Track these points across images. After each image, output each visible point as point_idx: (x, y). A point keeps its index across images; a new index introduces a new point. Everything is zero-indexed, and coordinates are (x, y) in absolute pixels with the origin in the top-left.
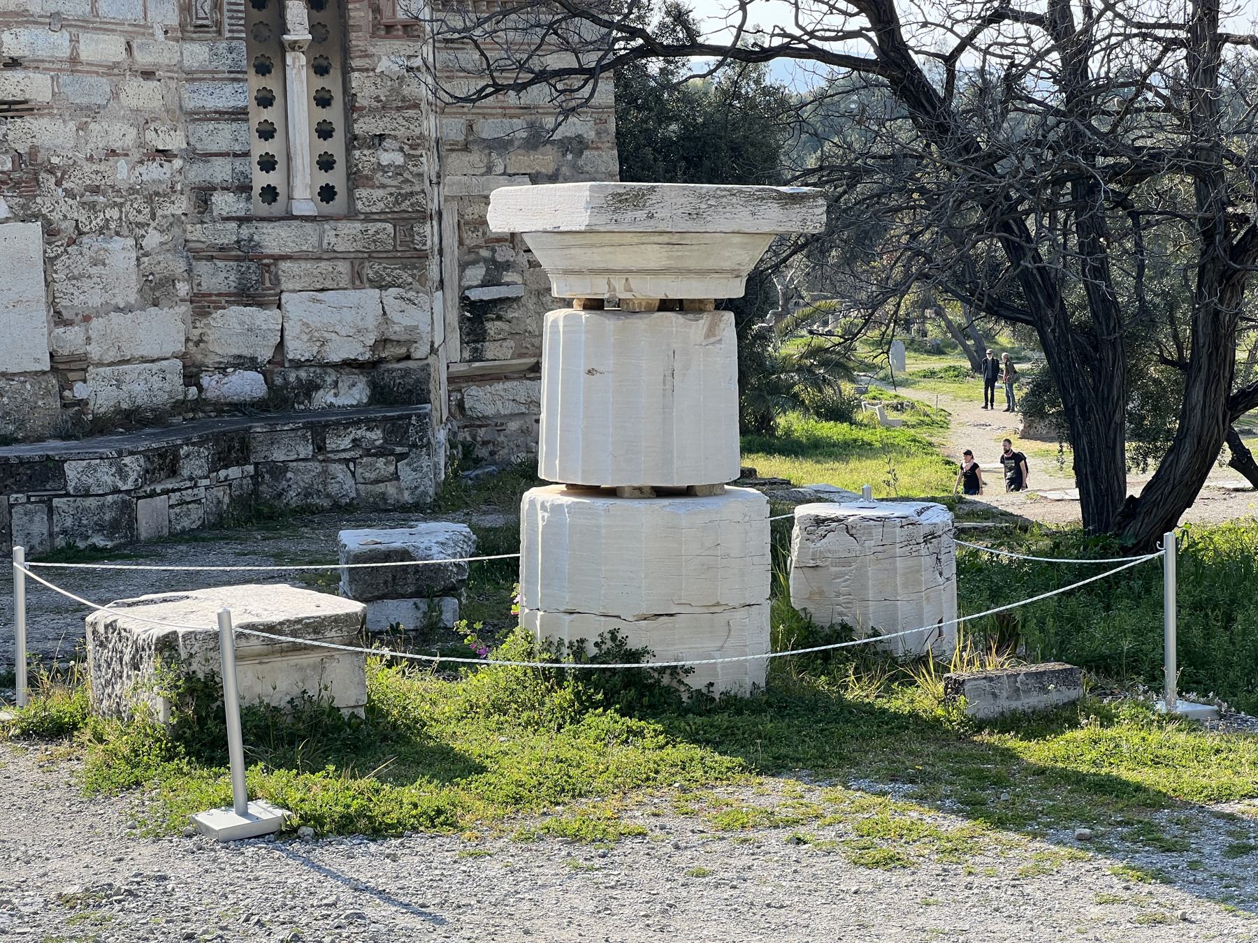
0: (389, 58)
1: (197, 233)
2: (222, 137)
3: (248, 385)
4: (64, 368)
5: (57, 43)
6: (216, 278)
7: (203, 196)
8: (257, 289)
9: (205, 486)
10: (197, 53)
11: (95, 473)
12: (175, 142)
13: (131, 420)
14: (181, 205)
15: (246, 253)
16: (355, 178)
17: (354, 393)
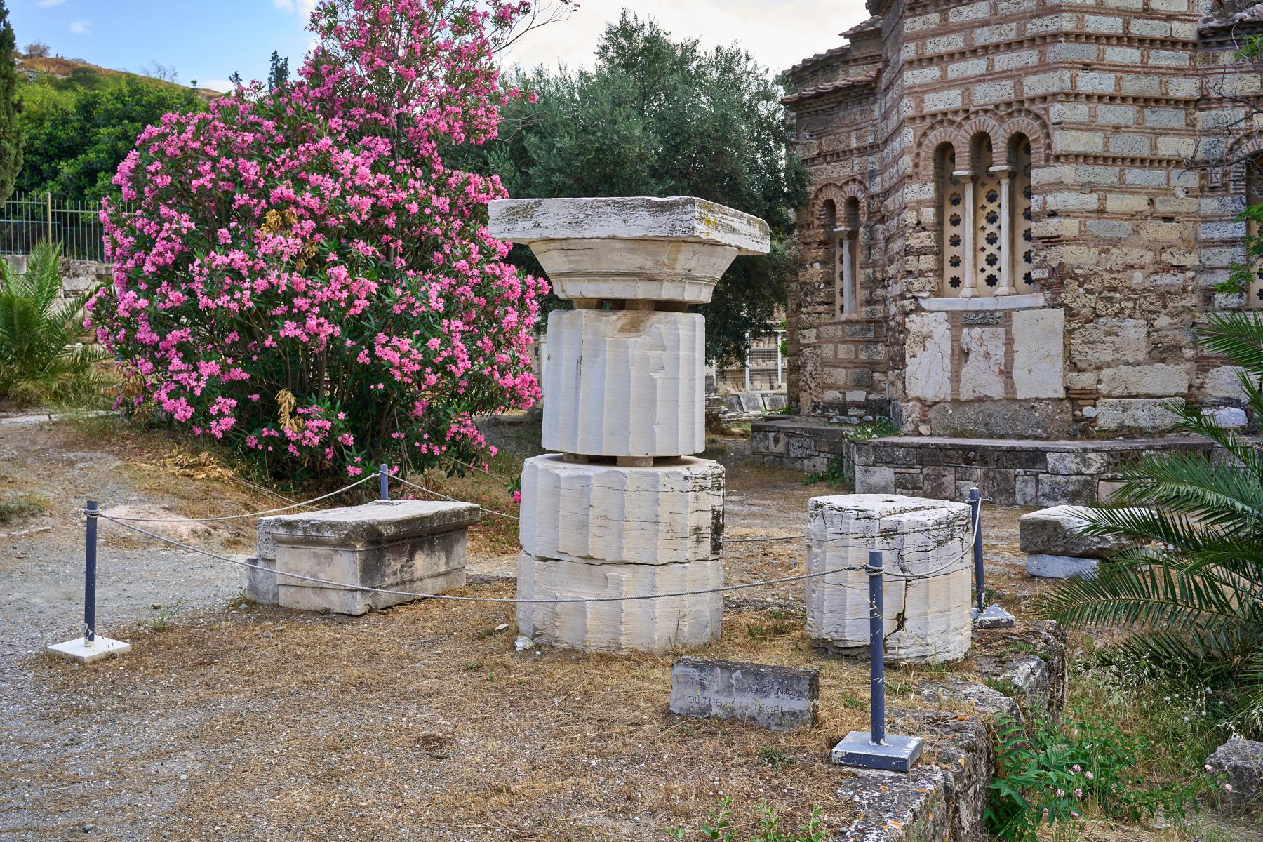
1: (1202, 318)
4: (1074, 397)
7: (1208, 296)
10: (1209, 205)
12: (1191, 260)
14: (1192, 300)
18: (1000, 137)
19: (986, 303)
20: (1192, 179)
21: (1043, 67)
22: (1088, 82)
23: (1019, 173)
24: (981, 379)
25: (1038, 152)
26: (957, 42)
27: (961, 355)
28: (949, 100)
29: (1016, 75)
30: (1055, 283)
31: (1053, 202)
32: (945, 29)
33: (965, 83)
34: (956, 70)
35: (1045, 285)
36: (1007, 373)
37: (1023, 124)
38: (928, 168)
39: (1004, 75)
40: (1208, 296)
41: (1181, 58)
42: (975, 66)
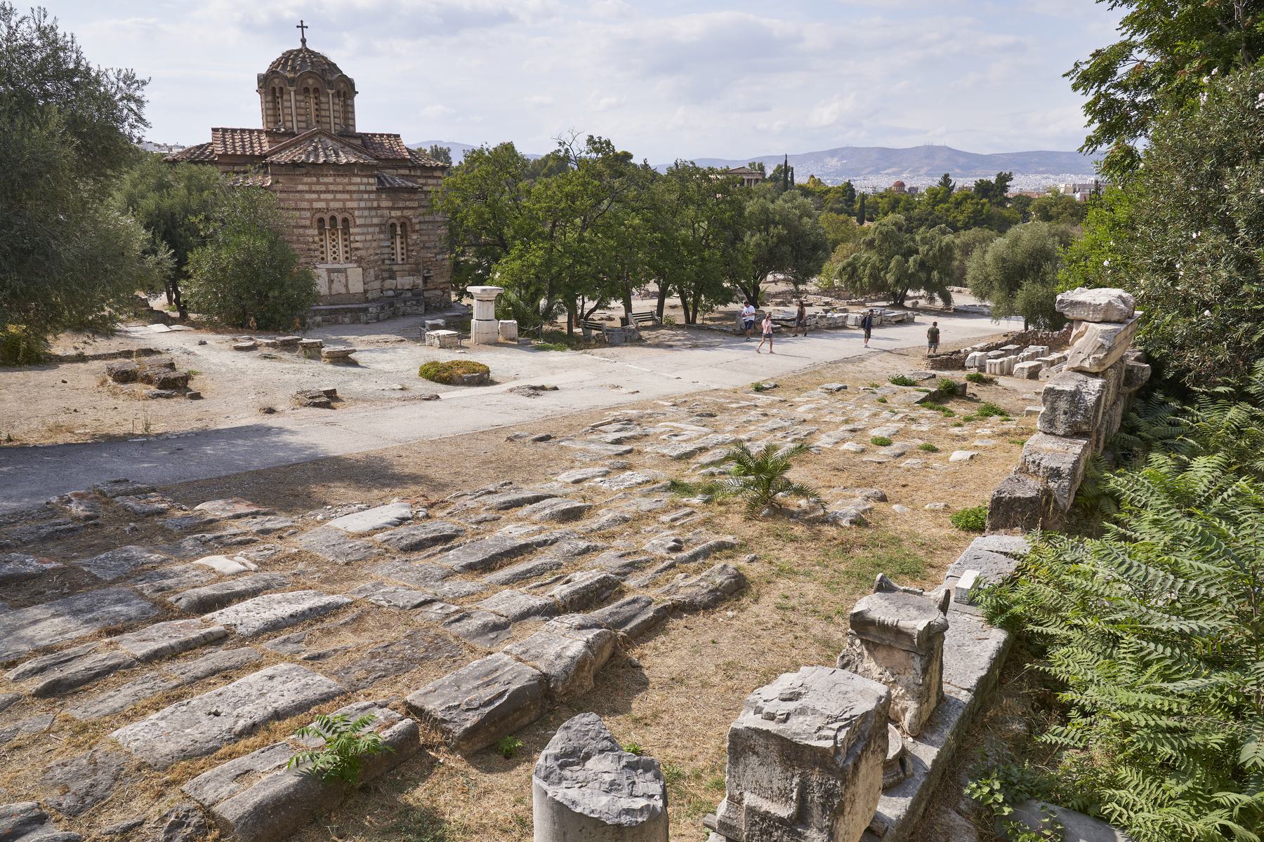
0: (415, 237)
2: (387, 250)
3: (391, 293)
4: (366, 291)
5: (363, 238)
6: (385, 275)
7: (383, 260)
8: (392, 277)
9: (388, 311)
10: (382, 236)
11: (373, 309)
13: (374, 300)
15: (391, 271)
16: (408, 257)
17: (409, 294)
18: (339, 218)
19: (336, 266)
20: (377, 229)
21: (351, 200)
22: (363, 204)
23: (346, 231)
24: (338, 288)
25: (351, 224)
26: (323, 188)
27: (331, 281)
28: (322, 205)
29: (344, 201)
30: (359, 261)
31: (358, 238)
32: (318, 183)
33: (327, 201)
34: (323, 196)
35: (356, 261)
36: (346, 286)
37: (347, 215)
38: (315, 225)
39: (339, 200)
40: (383, 260)
41: (373, 196)
42: (330, 196)
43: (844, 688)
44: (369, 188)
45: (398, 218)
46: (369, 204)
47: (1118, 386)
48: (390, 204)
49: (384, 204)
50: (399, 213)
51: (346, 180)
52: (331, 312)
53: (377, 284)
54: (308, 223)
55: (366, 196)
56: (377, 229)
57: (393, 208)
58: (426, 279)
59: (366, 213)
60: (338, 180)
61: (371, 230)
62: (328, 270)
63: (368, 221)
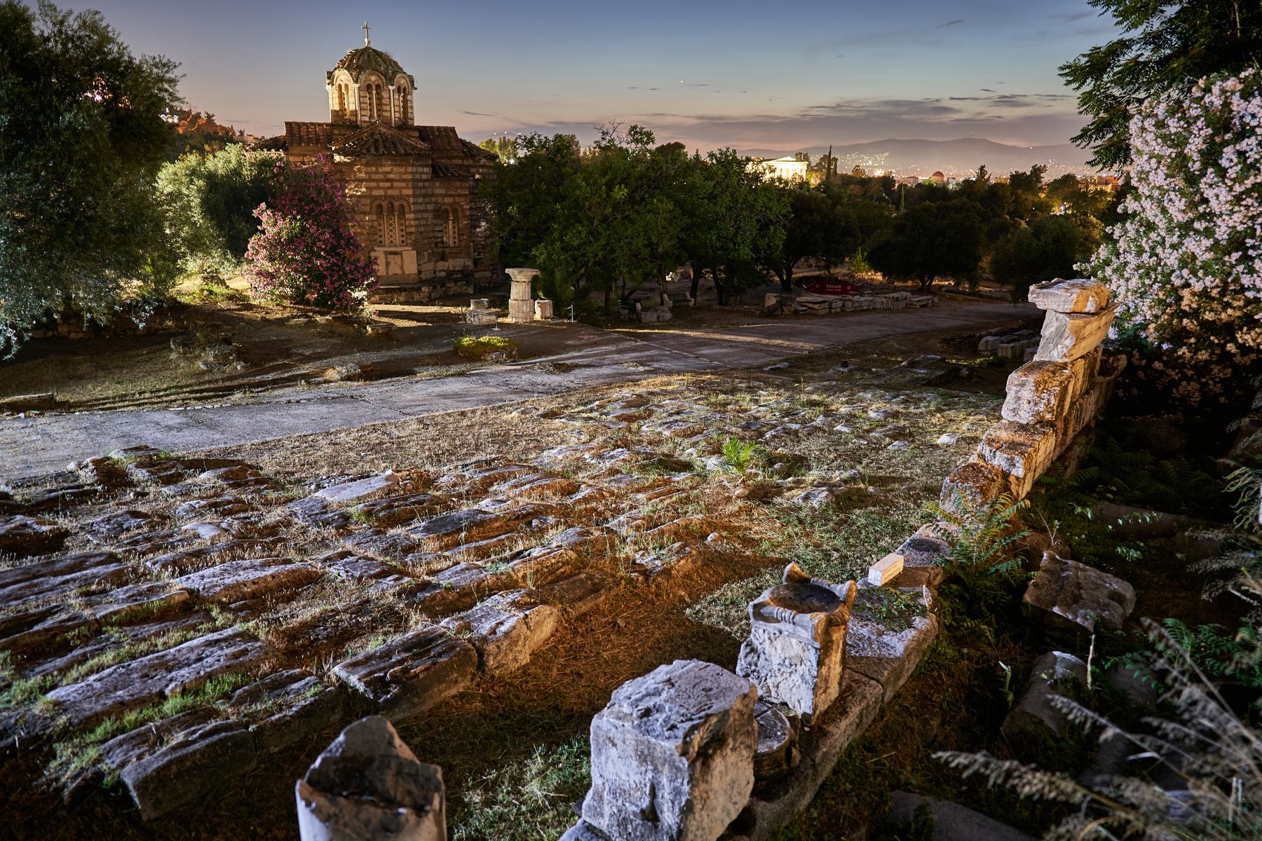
3: (443, 274)
21: (407, 188)
23: (402, 214)
24: (395, 269)
25: (407, 209)
27: (388, 264)
28: (381, 192)
30: (415, 246)
36: (402, 267)
38: (374, 210)
41: (427, 184)
43: (708, 685)
44: (424, 177)
45: (451, 205)
46: (423, 191)
47: (1091, 375)
48: (443, 191)
49: (438, 191)
50: (450, 200)
51: (403, 170)
52: (388, 291)
53: (430, 266)
54: (368, 209)
55: (421, 184)
56: (431, 215)
57: (446, 196)
58: (476, 262)
59: (420, 200)
60: (395, 169)
61: (425, 215)
62: (386, 253)
63: (423, 207)
